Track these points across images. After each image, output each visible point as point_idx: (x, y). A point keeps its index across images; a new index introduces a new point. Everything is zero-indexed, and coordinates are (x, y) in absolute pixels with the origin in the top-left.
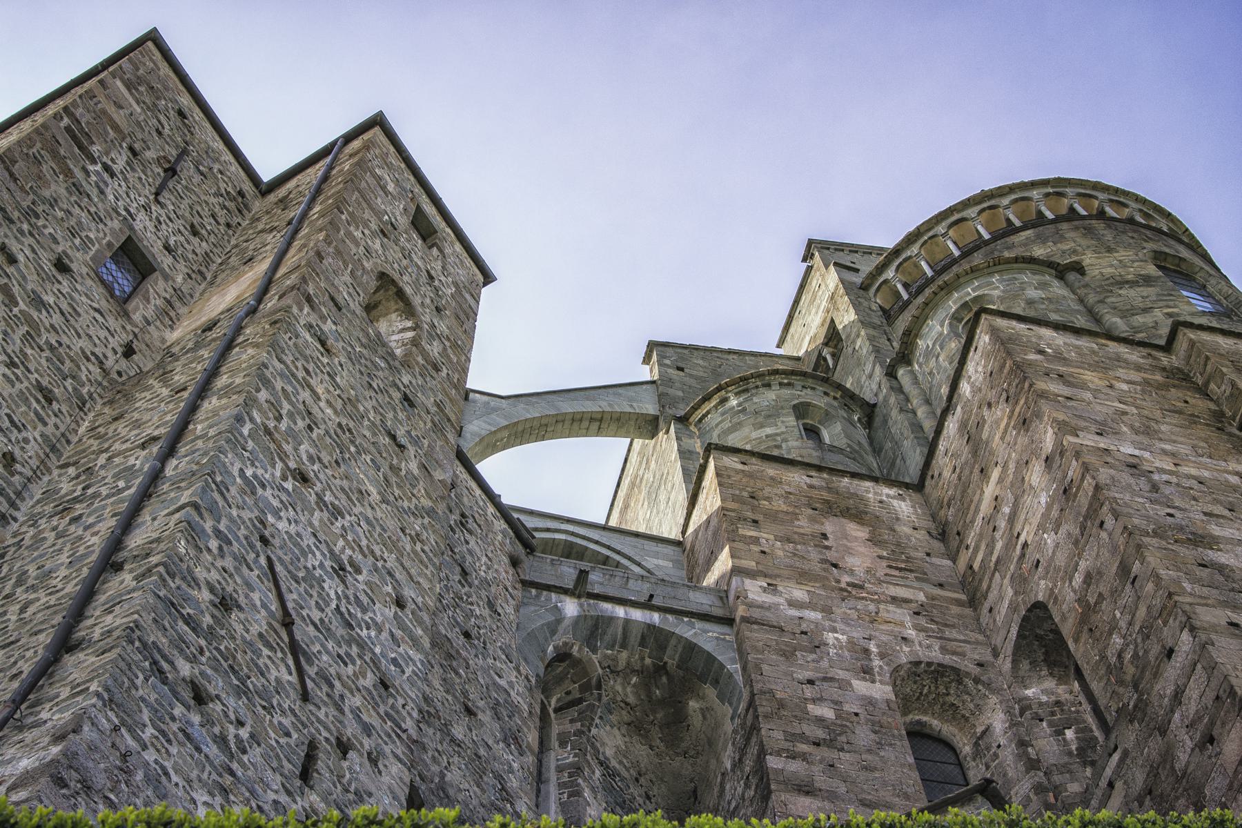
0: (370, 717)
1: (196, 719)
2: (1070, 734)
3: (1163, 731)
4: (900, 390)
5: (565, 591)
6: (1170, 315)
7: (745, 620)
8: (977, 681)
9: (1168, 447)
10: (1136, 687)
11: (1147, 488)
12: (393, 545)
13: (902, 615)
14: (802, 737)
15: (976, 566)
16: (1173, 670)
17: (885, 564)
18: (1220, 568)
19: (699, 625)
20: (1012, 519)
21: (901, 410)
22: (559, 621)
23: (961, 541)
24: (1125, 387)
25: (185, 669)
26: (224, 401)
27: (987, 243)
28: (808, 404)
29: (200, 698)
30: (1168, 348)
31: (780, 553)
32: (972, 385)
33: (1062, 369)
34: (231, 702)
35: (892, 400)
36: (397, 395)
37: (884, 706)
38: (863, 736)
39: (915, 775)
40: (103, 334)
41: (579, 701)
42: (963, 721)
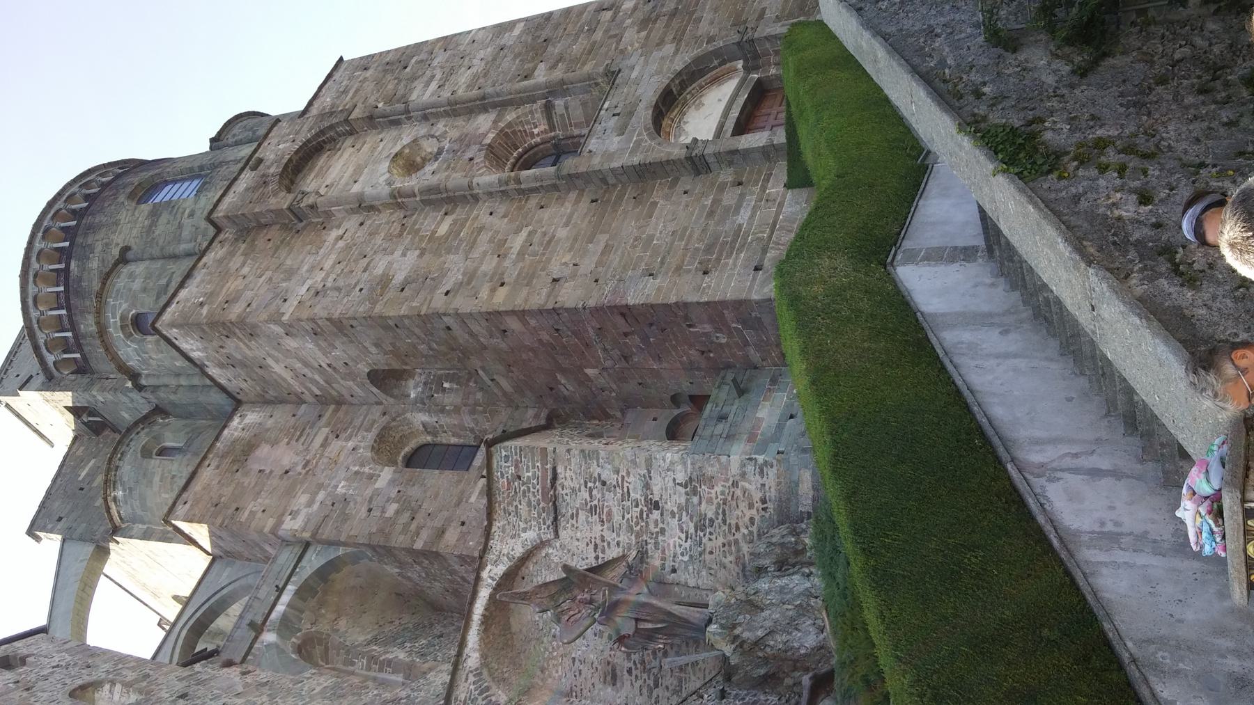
2: (446, 385)
3: (485, 348)
4: (155, 388)
5: (256, 638)
6: (191, 215)
7: (314, 535)
8: (394, 420)
9: (306, 268)
10: (453, 349)
13: (336, 445)
14: (406, 526)
15: (318, 393)
16: (457, 329)
17: (293, 442)
19: (303, 563)
20: (306, 364)
21: (175, 393)
22: (276, 646)
23: (296, 395)
24: (246, 270)
30: (219, 230)
31: (267, 501)
32: (198, 350)
37: (397, 475)
38: (415, 492)
39: (447, 472)
41: (327, 649)
42: (413, 434)
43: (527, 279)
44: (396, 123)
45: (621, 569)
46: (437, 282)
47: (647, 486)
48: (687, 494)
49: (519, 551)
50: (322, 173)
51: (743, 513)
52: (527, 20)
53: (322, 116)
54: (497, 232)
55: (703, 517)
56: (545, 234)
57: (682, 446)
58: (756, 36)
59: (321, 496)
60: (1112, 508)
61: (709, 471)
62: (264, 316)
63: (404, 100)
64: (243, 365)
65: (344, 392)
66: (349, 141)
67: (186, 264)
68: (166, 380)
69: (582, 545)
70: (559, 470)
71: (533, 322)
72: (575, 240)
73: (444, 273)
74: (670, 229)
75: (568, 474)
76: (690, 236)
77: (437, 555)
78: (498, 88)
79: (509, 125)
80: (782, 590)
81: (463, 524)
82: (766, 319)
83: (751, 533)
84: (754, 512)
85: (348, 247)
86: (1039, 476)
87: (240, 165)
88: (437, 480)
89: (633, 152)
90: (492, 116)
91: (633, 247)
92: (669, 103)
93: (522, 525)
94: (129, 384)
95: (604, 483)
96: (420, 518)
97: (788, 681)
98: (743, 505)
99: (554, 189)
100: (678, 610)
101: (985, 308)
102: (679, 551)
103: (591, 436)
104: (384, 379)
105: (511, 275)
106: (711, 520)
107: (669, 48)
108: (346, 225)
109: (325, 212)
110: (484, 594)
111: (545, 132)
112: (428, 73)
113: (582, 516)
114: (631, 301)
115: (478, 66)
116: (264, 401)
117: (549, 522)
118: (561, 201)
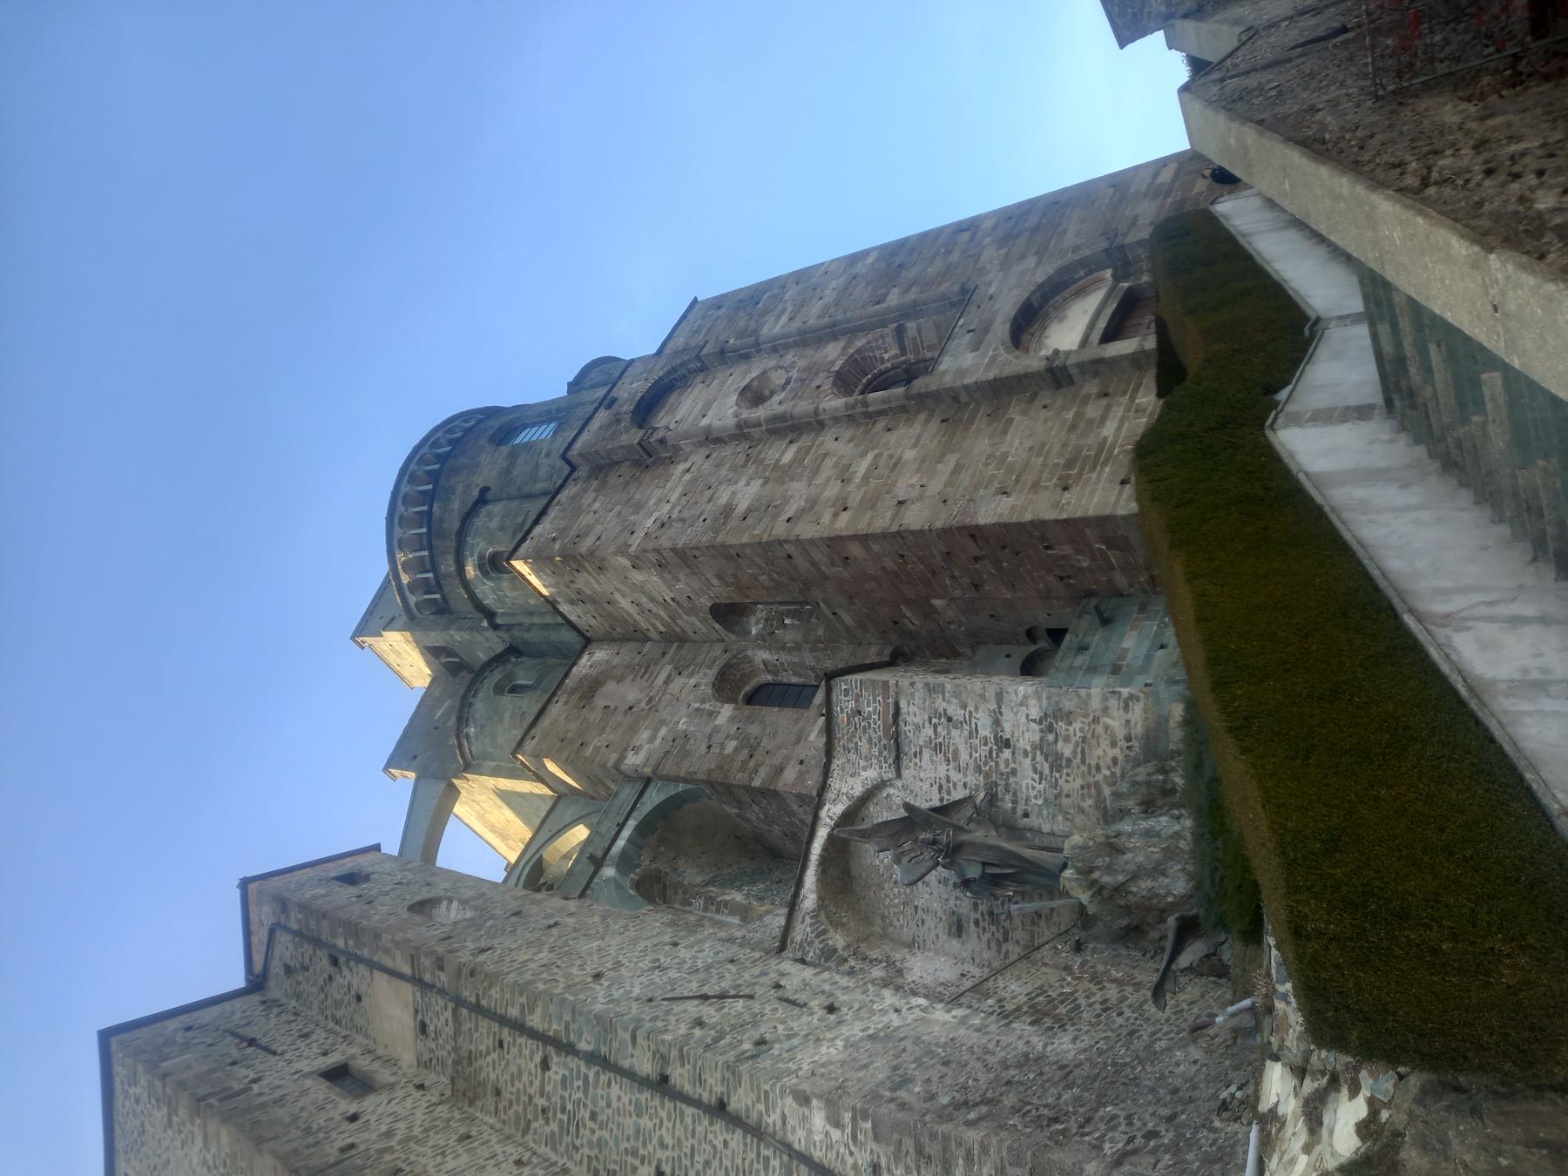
0: (757, 971)
1: (777, 1046)
3: (826, 578)
4: (509, 627)
6: (548, 455)
10: (794, 580)
11: (680, 525)
12: (634, 942)
13: (678, 682)
14: (744, 763)
16: (799, 560)
18: (749, 511)
19: (645, 798)
20: (652, 599)
21: (528, 631)
22: (616, 881)
24: (596, 506)
25: (747, 1046)
26: (539, 1011)
27: (429, 533)
28: (496, 685)
29: (761, 1042)
30: (573, 468)
33: (573, 533)
34: (763, 1030)
35: (516, 633)
36: (514, 919)
38: (754, 729)
39: (786, 710)
40: (409, 1101)
41: (665, 887)
43: (871, 503)
44: (746, 357)
45: (968, 811)
46: (779, 509)
47: (997, 723)
48: (1042, 731)
49: (858, 791)
50: (673, 411)
51: (1103, 752)
52: (881, 248)
53: (676, 353)
54: (842, 457)
55: (1058, 757)
56: (891, 457)
57: (1037, 680)
58: (1127, 241)
59: (663, 732)
60: (1541, 655)
61: (1067, 705)
62: (612, 549)
63: (755, 332)
64: (594, 602)
65: (688, 629)
66: (700, 378)
67: (543, 502)
68: (520, 619)
69: (926, 786)
70: (903, 704)
71: (876, 548)
72: (923, 460)
73: (786, 501)
74: (1027, 444)
75: (912, 708)
76: (1049, 451)
77: (775, 793)
78: (849, 314)
79: (859, 351)
80: (1147, 833)
81: (801, 762)
83: (1113, 774)
84: (1117, 751)
85: (694, 481)
86: (1443, 626)
87: (591, 408)
88: (779, 718)
89: (988, 367)
90: (842, 344)
91: (986, 465)
92: (1029, 320)
93: (862, 763)
94: (485, 624)
95: (950, 719)
96: (758, 755)
97: (1154, 934)
98: (1105, 744)
99: (902, 412)
100: (1028, 853)
101: (1382, 464)
102: (1033, 793)
103: (937, 672)
104: (728, 614)
105: (854, 500)
106: (1069, 761)
107: (1031, 261)
108: (693, 458)
109: (674, 446)
110: (822, 834)
111: (897, 356)
112: (780, 307)
113: (926, 754)
114: (981, 521)
115: (830, 295)
116: (609, 639)
117: (891, 761)
118: (909, 422)
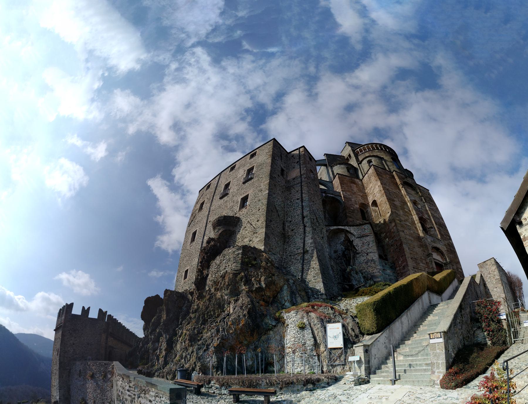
38: (356, 212)
43: (402, 226)
46: (397, 210)
49: (352, 232)
51: (370, 270)
73: (398, 211)
82: (405, 270)
